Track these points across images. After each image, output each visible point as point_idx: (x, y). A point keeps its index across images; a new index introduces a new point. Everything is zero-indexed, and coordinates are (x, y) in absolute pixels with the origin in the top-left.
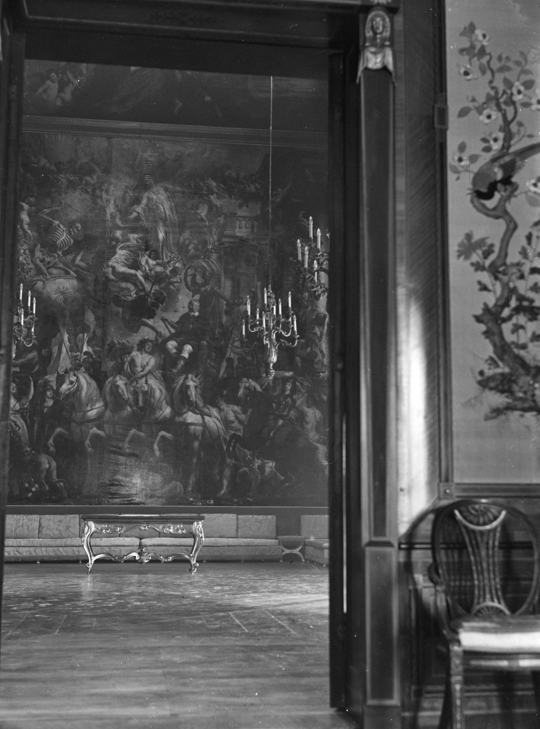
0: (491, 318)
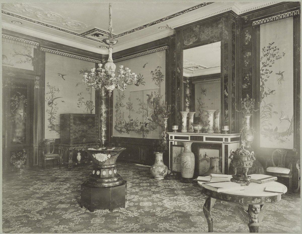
0: (50, 120)
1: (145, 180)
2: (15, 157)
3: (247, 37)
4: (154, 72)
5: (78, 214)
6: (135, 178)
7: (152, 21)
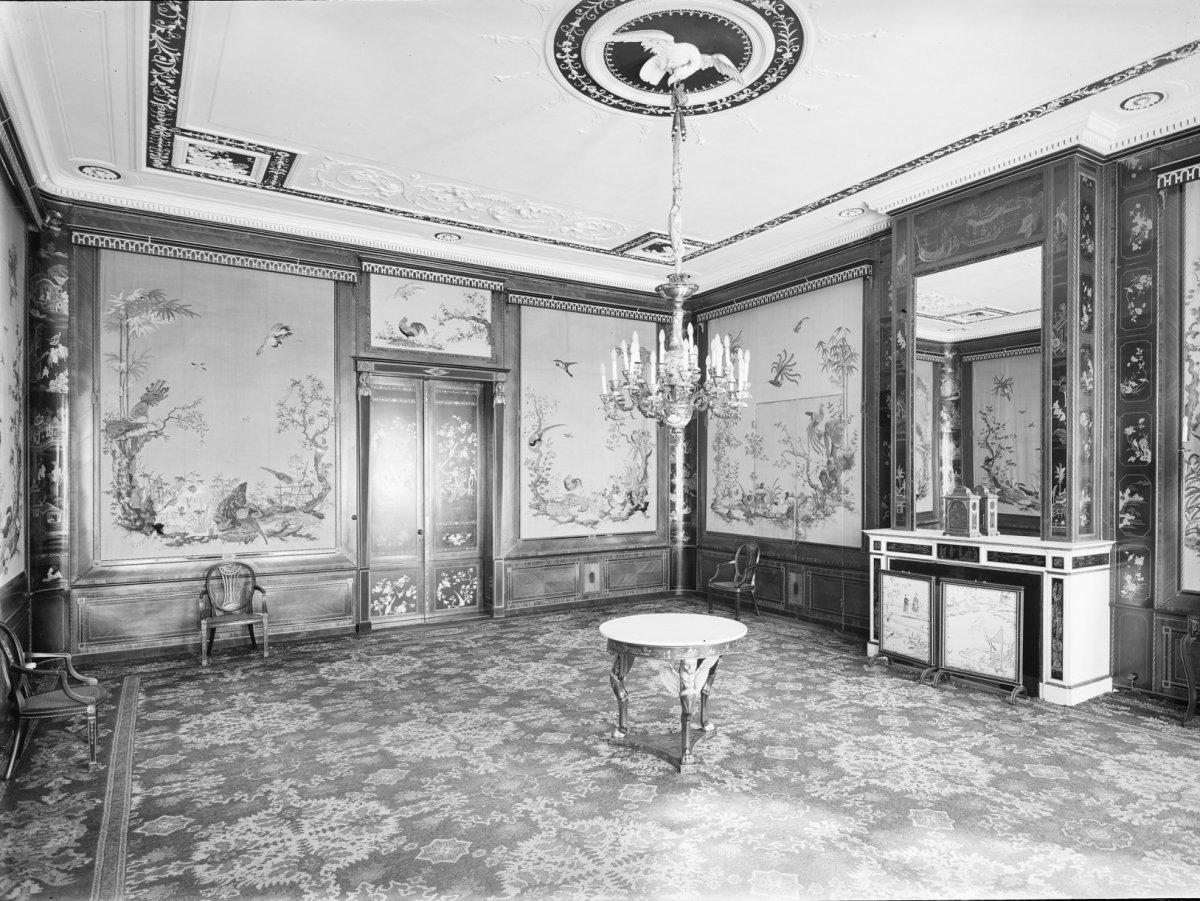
1: (792, 671)
2: (448, 584)
3: (1136, 224)
4: (829, 346)
5: (588, 767)
6: (762, 664)
7: (816, 199)
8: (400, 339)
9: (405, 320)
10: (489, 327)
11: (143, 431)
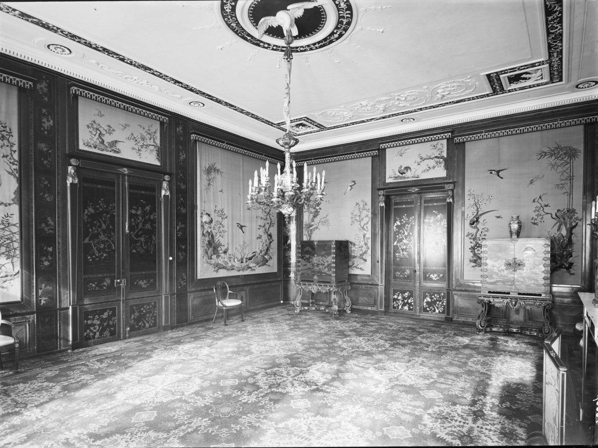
8: (398, 176)
9: (401, 167)
10: (446, 160)
11: (313, 227)
